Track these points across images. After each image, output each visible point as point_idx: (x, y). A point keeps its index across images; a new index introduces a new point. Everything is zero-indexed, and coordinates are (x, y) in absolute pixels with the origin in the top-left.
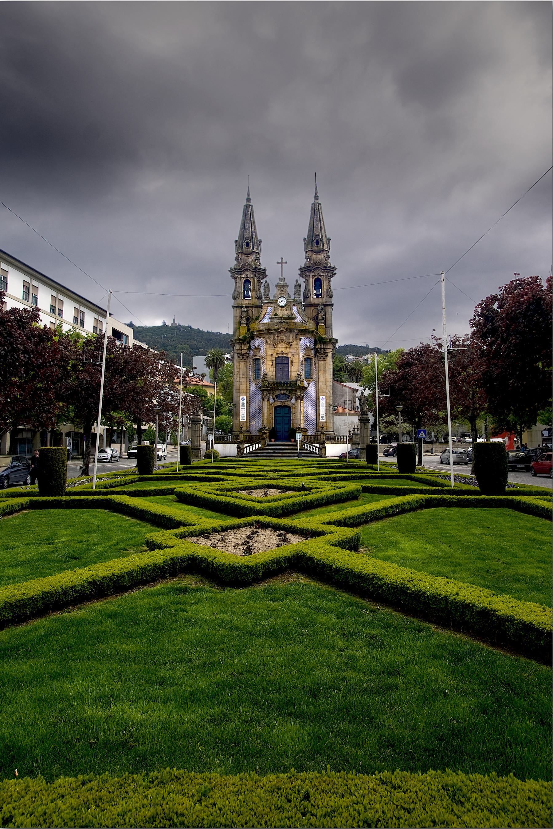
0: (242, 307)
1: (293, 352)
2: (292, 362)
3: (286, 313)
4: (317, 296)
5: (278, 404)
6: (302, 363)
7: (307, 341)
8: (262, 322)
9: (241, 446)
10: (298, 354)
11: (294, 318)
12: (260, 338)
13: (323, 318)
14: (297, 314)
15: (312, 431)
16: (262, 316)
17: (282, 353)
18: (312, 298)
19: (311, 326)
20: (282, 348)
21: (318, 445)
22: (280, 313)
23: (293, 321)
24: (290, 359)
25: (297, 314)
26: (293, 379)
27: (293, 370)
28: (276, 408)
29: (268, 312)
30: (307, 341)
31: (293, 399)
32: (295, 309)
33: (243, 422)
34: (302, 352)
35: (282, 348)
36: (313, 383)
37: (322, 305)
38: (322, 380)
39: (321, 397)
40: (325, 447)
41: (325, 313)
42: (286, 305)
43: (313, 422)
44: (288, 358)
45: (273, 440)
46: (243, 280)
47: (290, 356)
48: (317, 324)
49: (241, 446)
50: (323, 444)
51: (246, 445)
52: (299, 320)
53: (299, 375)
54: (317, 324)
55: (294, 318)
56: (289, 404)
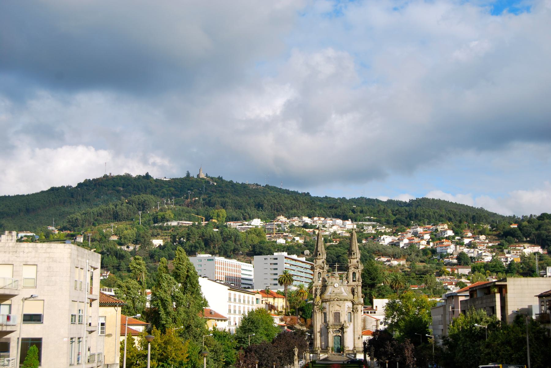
4: (353, 281)
5: (335, 335)
14: (344, 291)
18: (351, 282)
20: (336, 308)
21: (353, 355)
22: (336, 291)
25: (344, 291)
26: (343, 323)
32: (342, 289)
34: (346, 309)
36: (352, 324)
44: (339, 313)
46: (317, 273)
47: (340, 312)
48: (354, 295)
50: (355, 354)
52: (345, 294)
53: (345, 321)
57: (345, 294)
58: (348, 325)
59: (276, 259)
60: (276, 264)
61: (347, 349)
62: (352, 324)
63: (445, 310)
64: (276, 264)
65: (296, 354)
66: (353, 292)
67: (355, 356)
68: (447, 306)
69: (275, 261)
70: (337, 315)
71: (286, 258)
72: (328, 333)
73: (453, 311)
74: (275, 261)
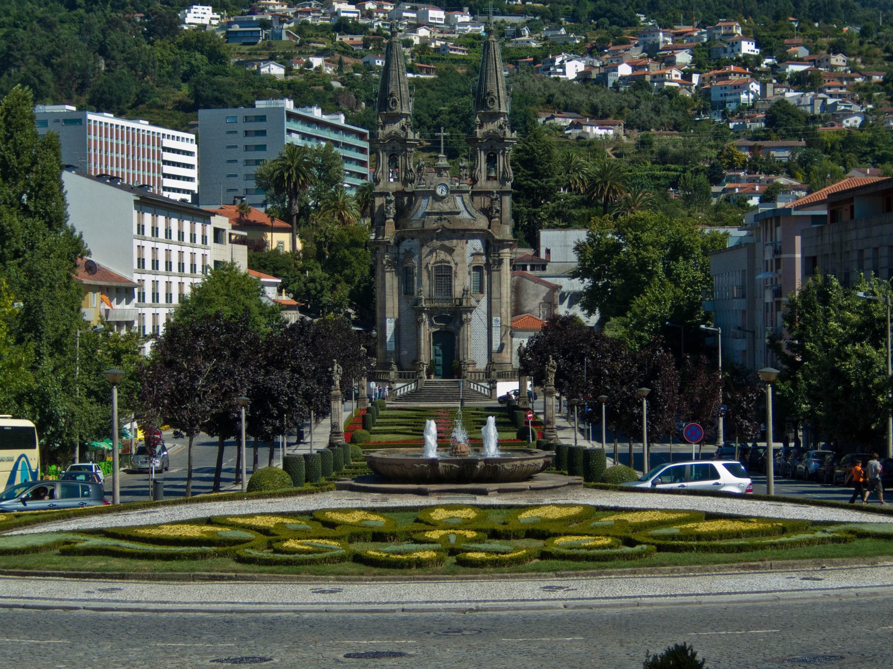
0: (387, 194)
1: (457, 259)
2: (456, 273)
3: (445, 207)
4: (489, 178)
6: (469, 274)
7: (477, 244)
8: (415, 218)
9: (392, 385)
10: (464, 262)
11: (458, 213)
12: (413, 239)
13: (497, 211)
14: (462, 208)
15: (482, 363)
16: (415, 210)
17: (443, 261)
19: (482, 222)
23: (457, 216)
24: (454, 269)
27: (457, 283)
28: (434, 333)
29: (424, 205)
30: (477, 244)
31: (458, 323)
32: (459, 199)
33: (391, 353)
34: (469, 259)
35: (443, 255)
37: (497, 192)
38: (495, 295)
39: (494, 318)
40: (495, 388)
41: (501, 202)
42: (447, 195)
43: (484, 351)
44: (451, 267)
45: (433, 376)
47: (453, 265)
49: (392, 385)
51: (398, 385)
53: (465, 291)
54: (490, 218)
55: (458, 213)
56: (451, 327)
57: (465, 215)
58: (473, 302)
59: (262, 118)
60: (263, 133)
61: (470, 369)
62: (484, 300)
63: (752, 256)
64: (263, 133)
65: (338, 382)
66: (487, 212)
67: (493, 389)
68: (759, 247)
69: (260, 126)
70: (444, 274)
71: (290, 115)
72: (418, 324)
73: (778, 261)
74: (260, 126)
